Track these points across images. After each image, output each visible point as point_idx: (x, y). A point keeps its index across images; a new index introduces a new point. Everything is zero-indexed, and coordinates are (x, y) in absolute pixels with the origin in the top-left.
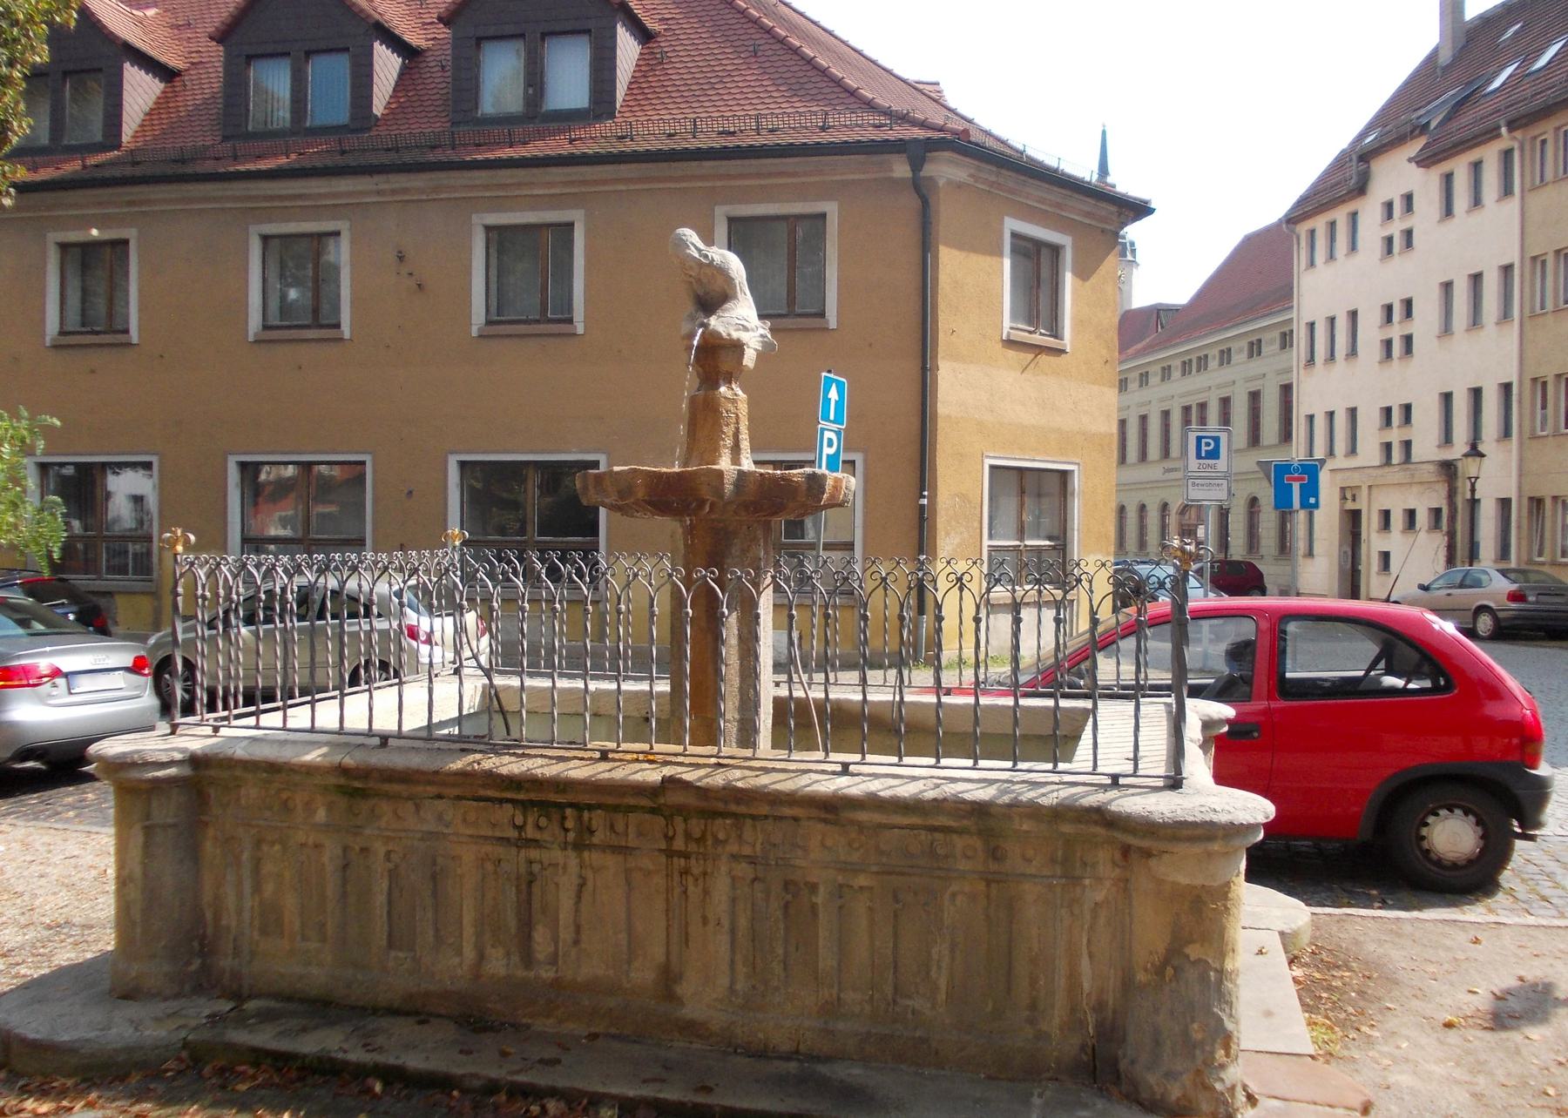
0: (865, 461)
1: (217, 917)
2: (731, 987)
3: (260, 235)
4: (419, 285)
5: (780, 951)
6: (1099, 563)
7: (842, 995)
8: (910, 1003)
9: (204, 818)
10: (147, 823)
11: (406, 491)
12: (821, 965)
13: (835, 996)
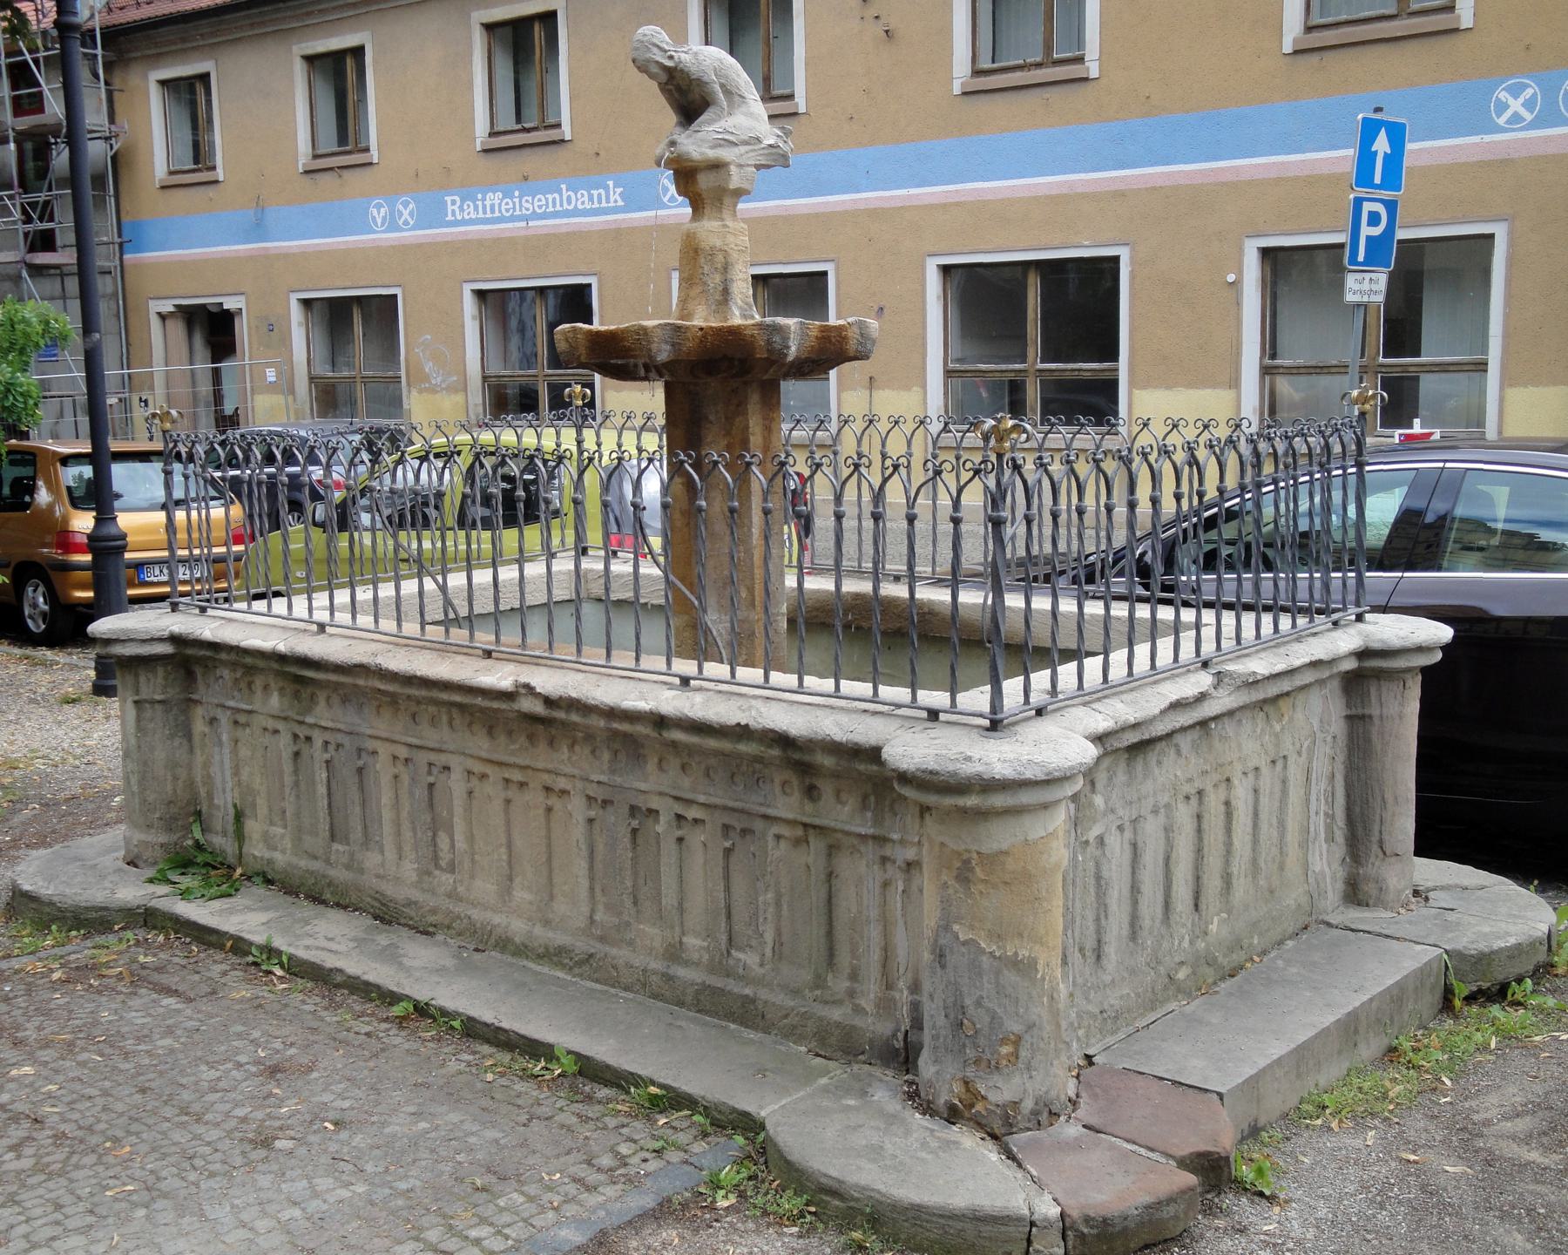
0: (1511, 235)
1: (210, 796)
2: (591, 917)
3: (482, 24)
4: (887, 32)
5: (629, 883)
6: (1199, 424)
7: (685, 939)
8: (741, 956)
9: (194, 697)
10: (136, 698)
11: (876, 308)
12: (664, 902)
13: (677, 939)
